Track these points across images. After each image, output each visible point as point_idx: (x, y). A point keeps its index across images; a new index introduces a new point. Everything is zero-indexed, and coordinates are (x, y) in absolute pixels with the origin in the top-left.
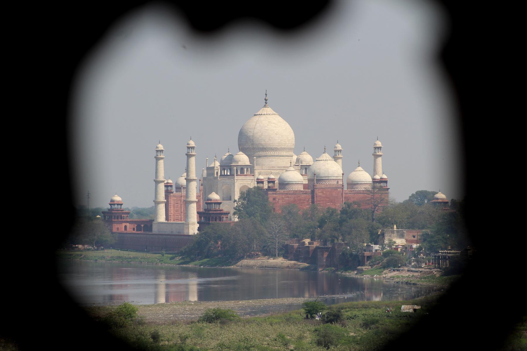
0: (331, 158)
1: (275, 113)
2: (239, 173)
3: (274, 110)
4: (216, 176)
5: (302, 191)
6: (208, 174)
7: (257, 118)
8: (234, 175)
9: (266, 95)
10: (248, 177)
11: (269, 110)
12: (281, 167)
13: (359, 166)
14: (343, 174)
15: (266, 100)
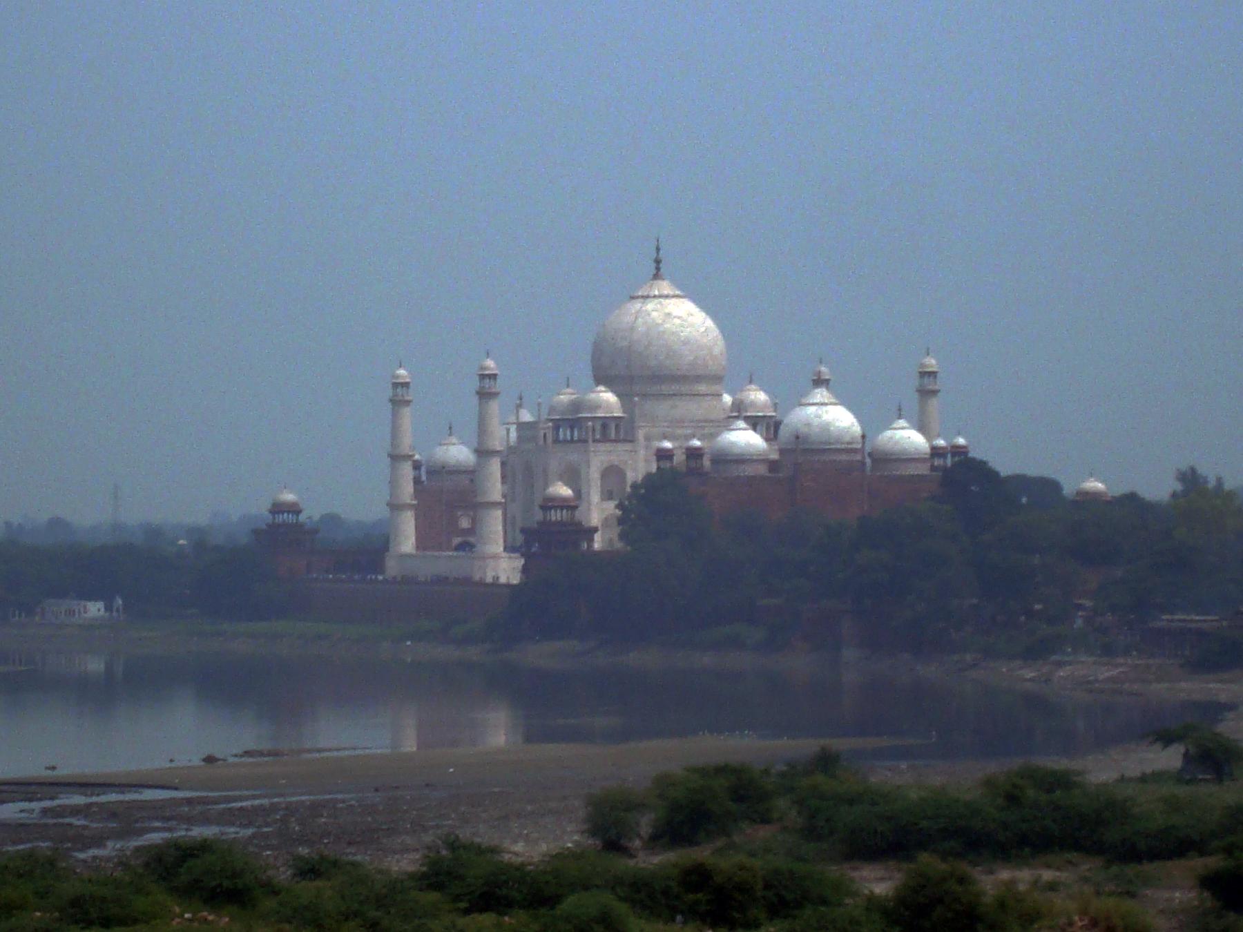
0: (833, 400)
1: (678, 292)
2: (598, 437)
3: (679, 287)
4: (541, 442)
5: (763, 478)
6: (519, 437)
7: (637, 305)
8: (585, 441)
9: (658, 249)
10: (621, 447)
11: (665, 287)
12: (699, 421)
13: (900, 418)
14: (863, 437)
15: (658, 262)
